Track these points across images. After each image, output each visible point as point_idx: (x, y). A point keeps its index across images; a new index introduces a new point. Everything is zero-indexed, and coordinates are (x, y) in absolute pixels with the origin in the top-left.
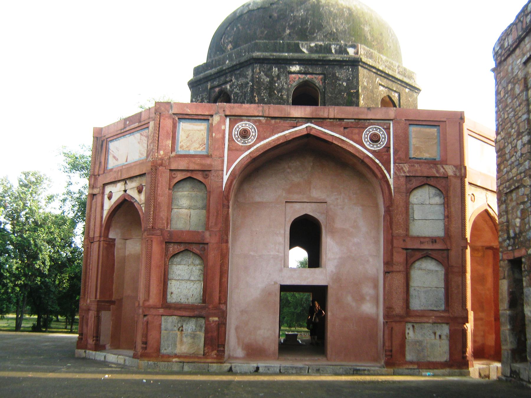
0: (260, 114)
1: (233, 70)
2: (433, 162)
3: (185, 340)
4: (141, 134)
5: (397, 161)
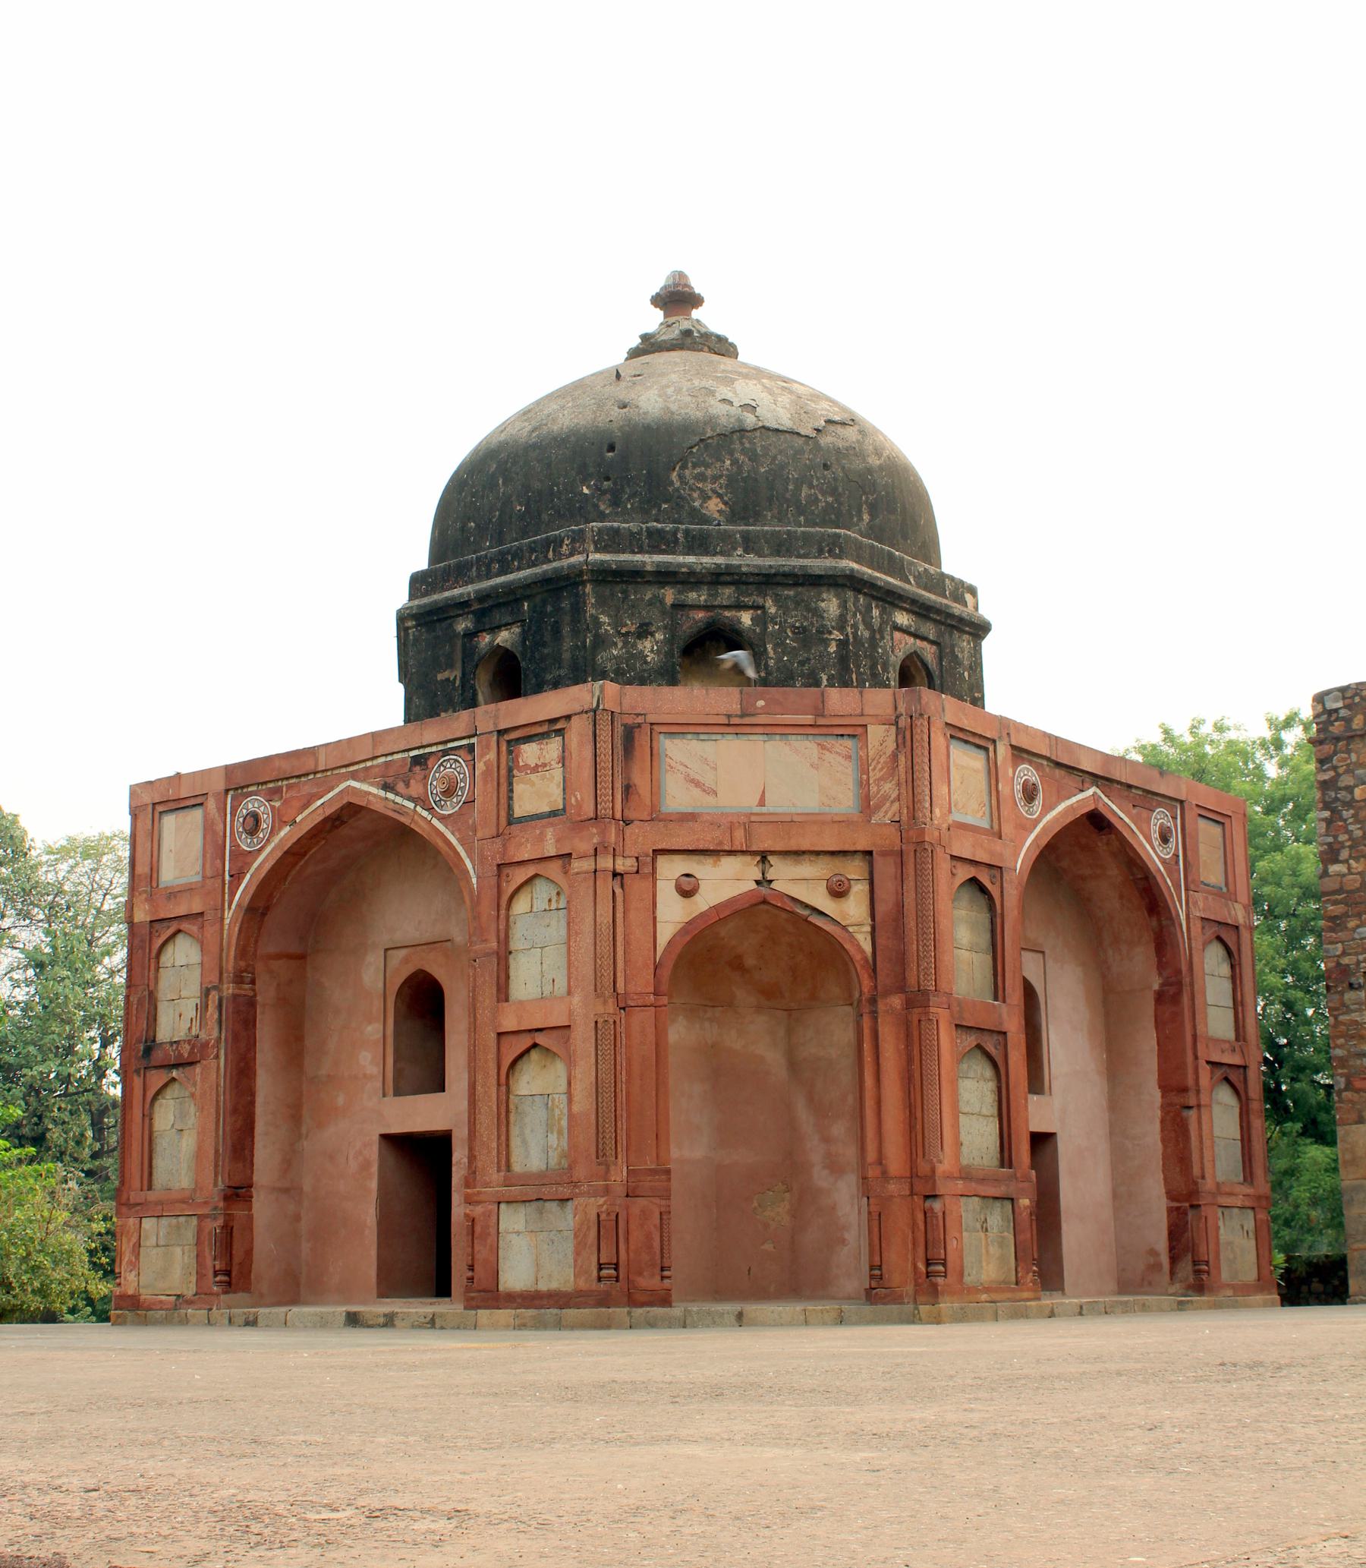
1: (767, 581)
2: (1218, 893)
3: (992, 1250)
4: (823, 747)
5: (1192, 887)
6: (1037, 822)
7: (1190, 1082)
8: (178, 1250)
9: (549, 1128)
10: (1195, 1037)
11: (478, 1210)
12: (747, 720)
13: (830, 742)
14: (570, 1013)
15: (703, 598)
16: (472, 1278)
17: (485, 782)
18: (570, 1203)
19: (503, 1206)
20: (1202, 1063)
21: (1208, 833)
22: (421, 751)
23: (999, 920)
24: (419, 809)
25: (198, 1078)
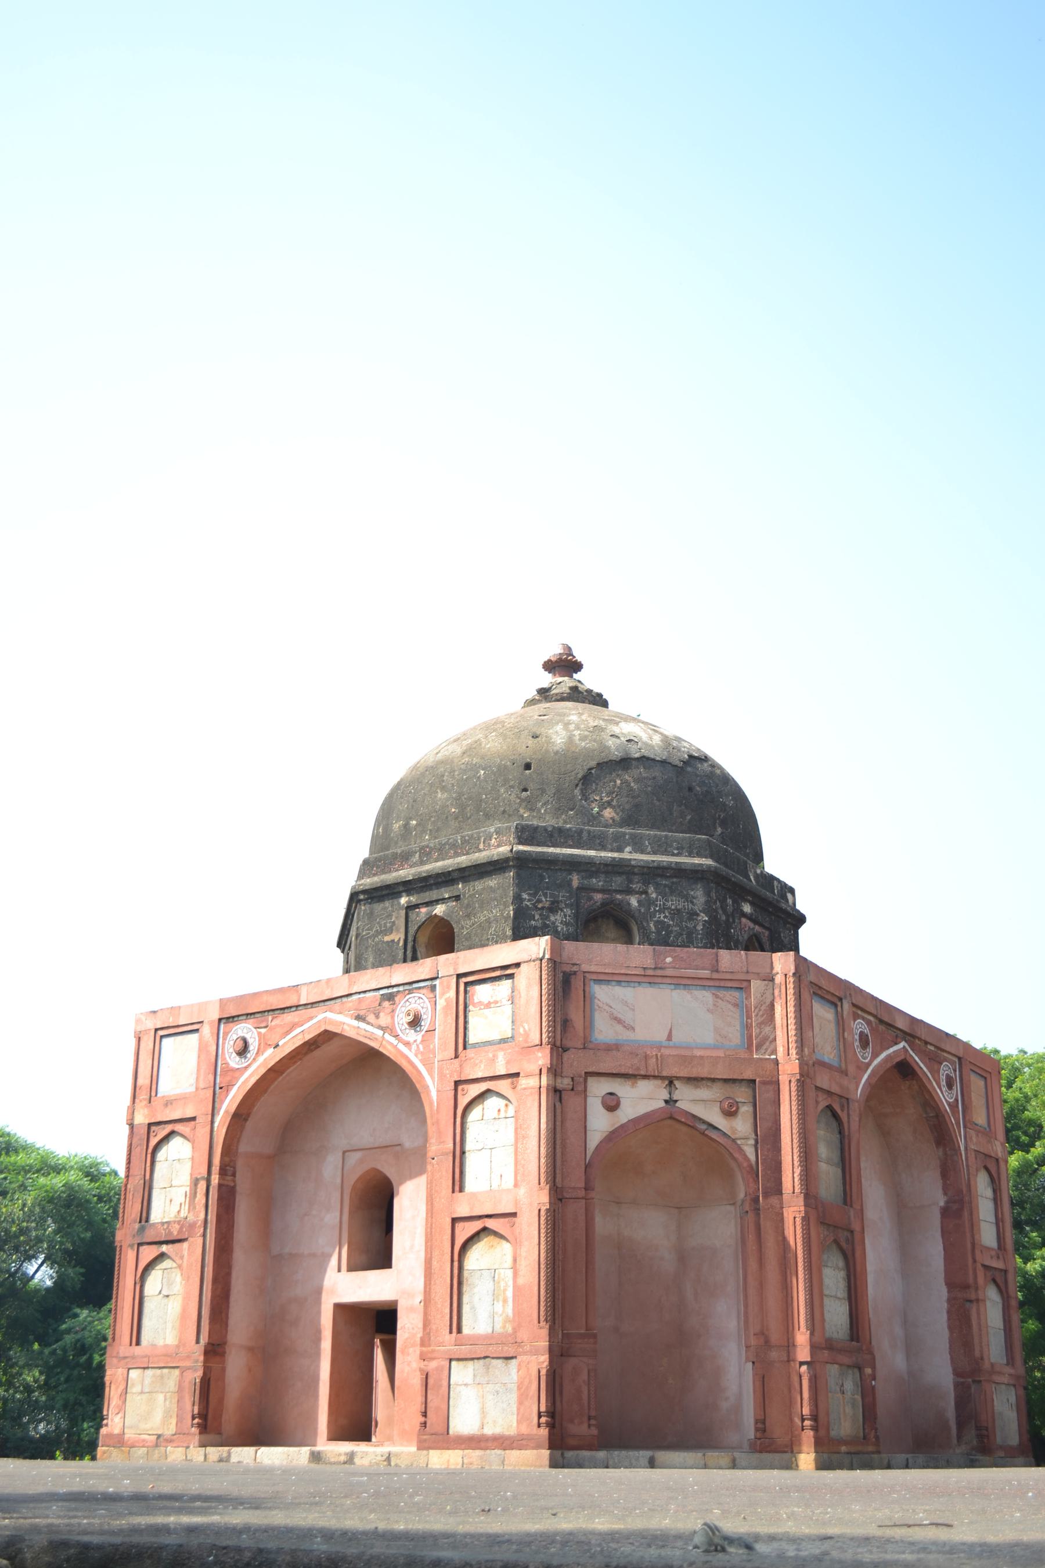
0: (873, 1011)
1: (652, 873)
4: (717, 997)
6: (868, 1065)
7: (971, 1281)
8: (161, 1397)
9: (495, 1297)
10: (973, 1244)
11: (433, 1364)
12: (659, 972)
13: (721, 993)
14: (516, 1202)
15: (600, 884)
16: (425, 1423)
17: (446, 1015)
18: (514, 1361)
19: (454, 1363)
20: (979, 1266)
21: (977, 1084)
22: (390, 990)
23: (847, 1141)
24: (387, 1036)
25: (185, 1253)
